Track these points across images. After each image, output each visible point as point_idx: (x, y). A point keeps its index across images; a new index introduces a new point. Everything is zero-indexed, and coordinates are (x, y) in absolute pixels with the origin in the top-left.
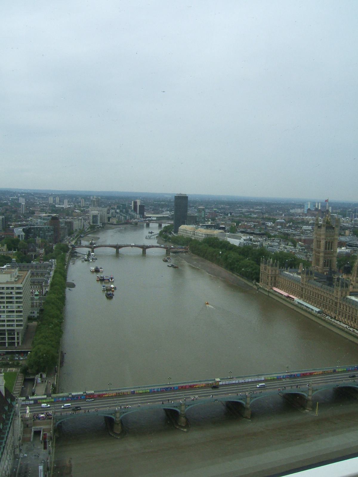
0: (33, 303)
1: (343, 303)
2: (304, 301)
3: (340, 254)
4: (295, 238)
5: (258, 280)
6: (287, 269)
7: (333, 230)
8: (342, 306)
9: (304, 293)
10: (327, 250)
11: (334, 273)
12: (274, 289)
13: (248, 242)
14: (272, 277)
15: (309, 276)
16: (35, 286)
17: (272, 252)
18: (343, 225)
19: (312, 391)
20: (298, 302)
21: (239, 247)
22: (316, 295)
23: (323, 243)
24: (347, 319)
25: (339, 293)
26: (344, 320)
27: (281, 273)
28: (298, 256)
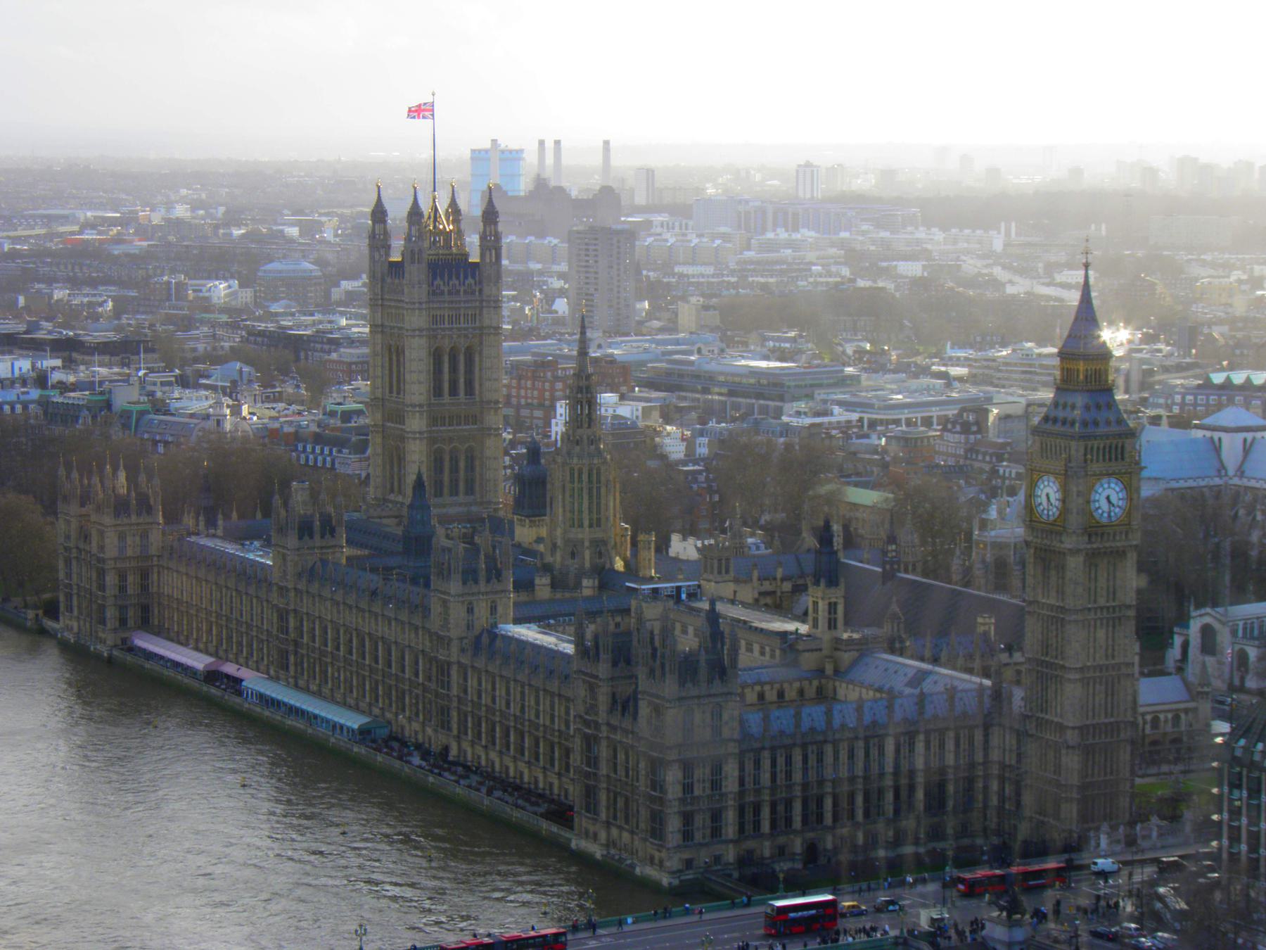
1: (476, 665)
2: (296, 686)
4: (334, 356)
6: (211, 523)
7: (470, 281)
8: (472, 683)
9: (296, 644)
10: (446, 398)
13: (22, 398)
14: (122, 576)
15: (317, 541)
17: (155, 443)
18: (681, 276)
22: (351, 641)
24: (498, 748)
25: (458, 613)
26: (487, 754)
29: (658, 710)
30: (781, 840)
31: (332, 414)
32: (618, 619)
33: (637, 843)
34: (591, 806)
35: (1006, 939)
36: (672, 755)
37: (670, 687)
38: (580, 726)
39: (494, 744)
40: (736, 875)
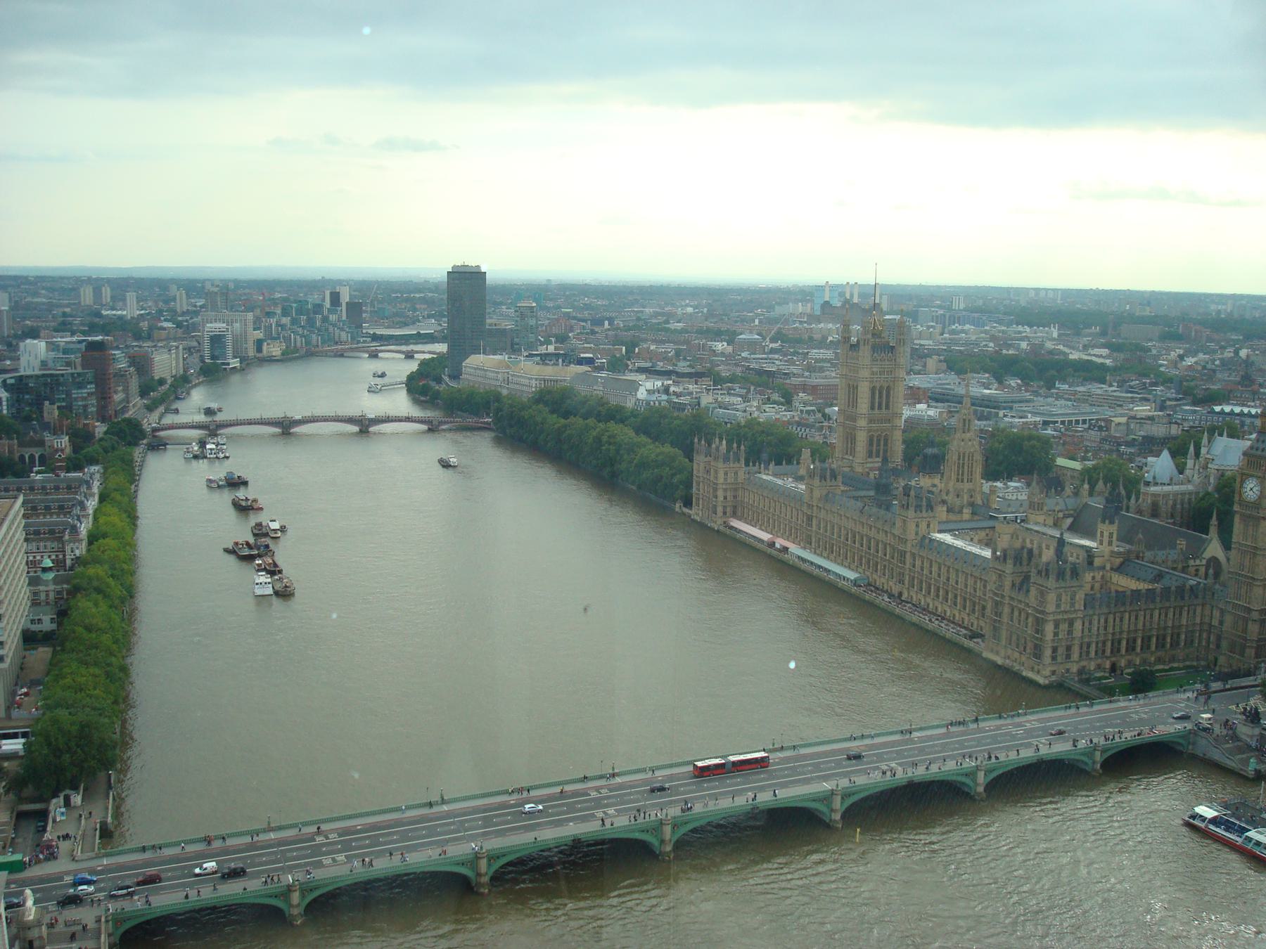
0: (35, 594)
2: (815, 553)
3: (912, 423)
4: (788, 381)
5: (688, 503)
6: (767, 468)
7: (890, 354)
8: (918, 563)
9: (817, 533)
10: (876, 411)
11: (896, 472)
12: (732, 524)
16: (42, 544)
19: (842, 798)
20: (799, 557)
21: (634, 414)
22: (848, 534)
23: (864, 390)
27: (749, 479)
28: (802, 432)
29: (1042, 594)
30: (1099, 661)
31: (802, 411)
32: (987, 531)
33: (1024, 659)
34: (996, 637)
35: (1250, 733)
36: (1051, 617)
37: (1051, 583)
38: (991, 595)
39: (929, 593)
40: (1076, 679)
